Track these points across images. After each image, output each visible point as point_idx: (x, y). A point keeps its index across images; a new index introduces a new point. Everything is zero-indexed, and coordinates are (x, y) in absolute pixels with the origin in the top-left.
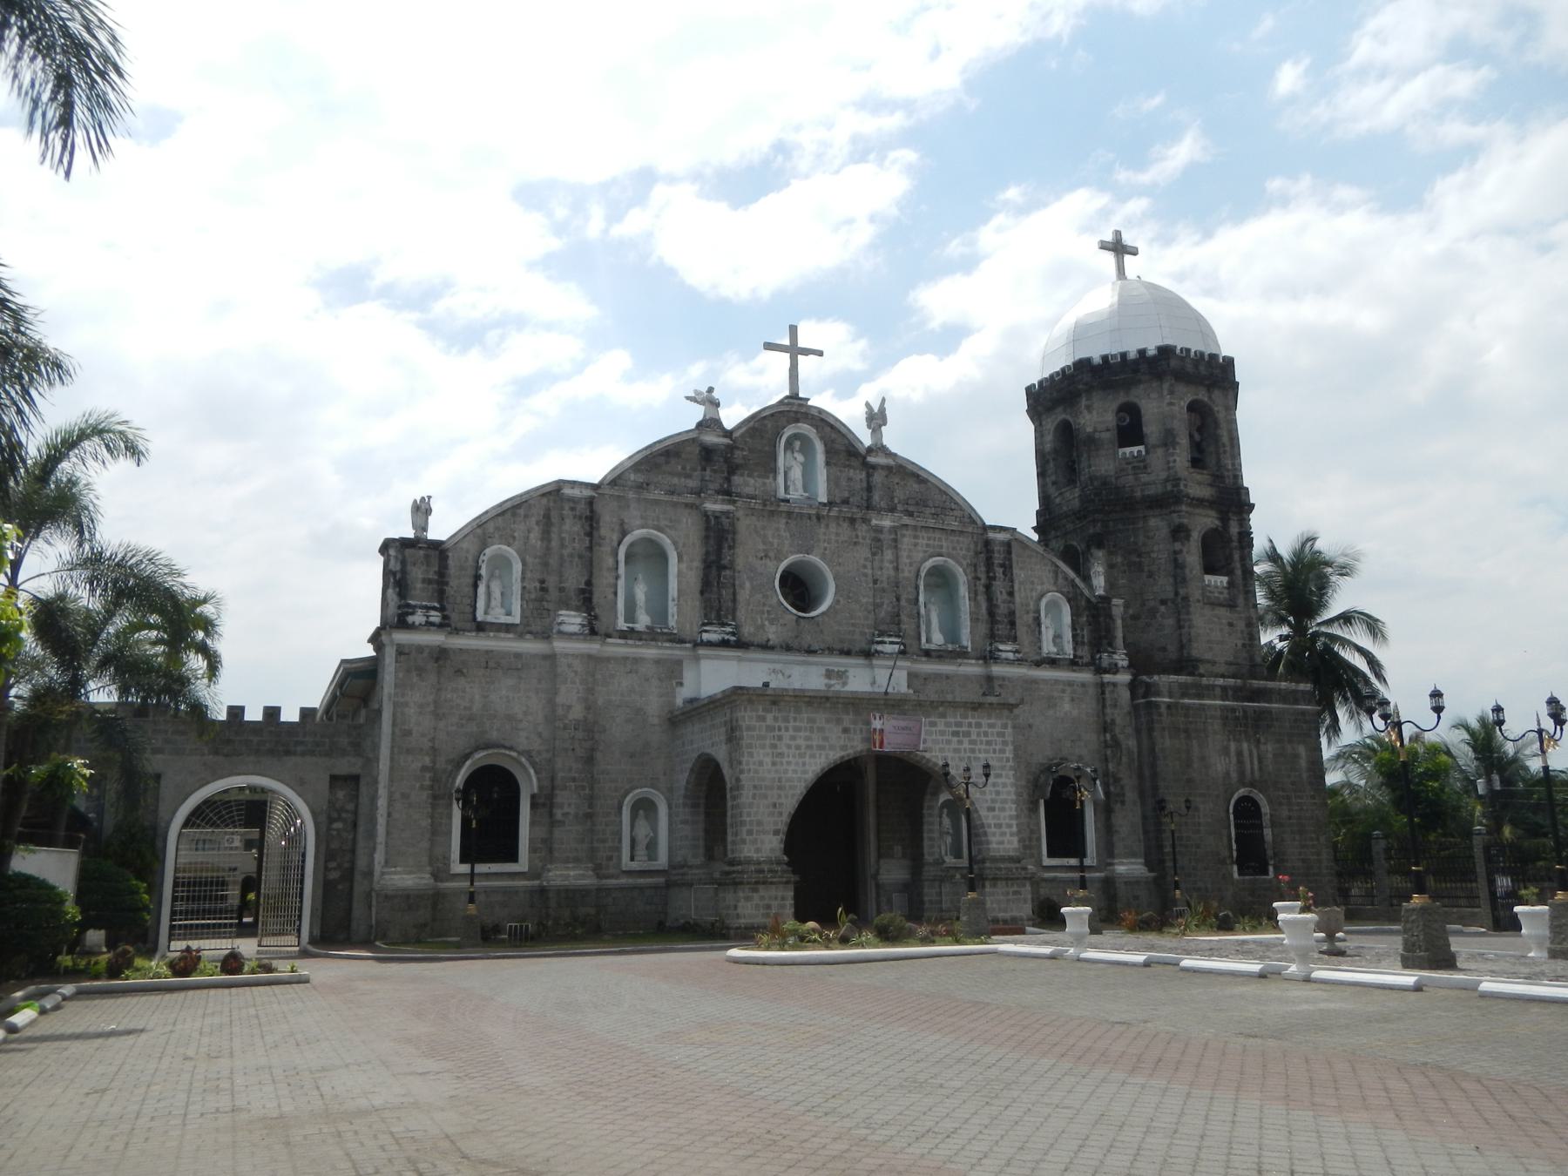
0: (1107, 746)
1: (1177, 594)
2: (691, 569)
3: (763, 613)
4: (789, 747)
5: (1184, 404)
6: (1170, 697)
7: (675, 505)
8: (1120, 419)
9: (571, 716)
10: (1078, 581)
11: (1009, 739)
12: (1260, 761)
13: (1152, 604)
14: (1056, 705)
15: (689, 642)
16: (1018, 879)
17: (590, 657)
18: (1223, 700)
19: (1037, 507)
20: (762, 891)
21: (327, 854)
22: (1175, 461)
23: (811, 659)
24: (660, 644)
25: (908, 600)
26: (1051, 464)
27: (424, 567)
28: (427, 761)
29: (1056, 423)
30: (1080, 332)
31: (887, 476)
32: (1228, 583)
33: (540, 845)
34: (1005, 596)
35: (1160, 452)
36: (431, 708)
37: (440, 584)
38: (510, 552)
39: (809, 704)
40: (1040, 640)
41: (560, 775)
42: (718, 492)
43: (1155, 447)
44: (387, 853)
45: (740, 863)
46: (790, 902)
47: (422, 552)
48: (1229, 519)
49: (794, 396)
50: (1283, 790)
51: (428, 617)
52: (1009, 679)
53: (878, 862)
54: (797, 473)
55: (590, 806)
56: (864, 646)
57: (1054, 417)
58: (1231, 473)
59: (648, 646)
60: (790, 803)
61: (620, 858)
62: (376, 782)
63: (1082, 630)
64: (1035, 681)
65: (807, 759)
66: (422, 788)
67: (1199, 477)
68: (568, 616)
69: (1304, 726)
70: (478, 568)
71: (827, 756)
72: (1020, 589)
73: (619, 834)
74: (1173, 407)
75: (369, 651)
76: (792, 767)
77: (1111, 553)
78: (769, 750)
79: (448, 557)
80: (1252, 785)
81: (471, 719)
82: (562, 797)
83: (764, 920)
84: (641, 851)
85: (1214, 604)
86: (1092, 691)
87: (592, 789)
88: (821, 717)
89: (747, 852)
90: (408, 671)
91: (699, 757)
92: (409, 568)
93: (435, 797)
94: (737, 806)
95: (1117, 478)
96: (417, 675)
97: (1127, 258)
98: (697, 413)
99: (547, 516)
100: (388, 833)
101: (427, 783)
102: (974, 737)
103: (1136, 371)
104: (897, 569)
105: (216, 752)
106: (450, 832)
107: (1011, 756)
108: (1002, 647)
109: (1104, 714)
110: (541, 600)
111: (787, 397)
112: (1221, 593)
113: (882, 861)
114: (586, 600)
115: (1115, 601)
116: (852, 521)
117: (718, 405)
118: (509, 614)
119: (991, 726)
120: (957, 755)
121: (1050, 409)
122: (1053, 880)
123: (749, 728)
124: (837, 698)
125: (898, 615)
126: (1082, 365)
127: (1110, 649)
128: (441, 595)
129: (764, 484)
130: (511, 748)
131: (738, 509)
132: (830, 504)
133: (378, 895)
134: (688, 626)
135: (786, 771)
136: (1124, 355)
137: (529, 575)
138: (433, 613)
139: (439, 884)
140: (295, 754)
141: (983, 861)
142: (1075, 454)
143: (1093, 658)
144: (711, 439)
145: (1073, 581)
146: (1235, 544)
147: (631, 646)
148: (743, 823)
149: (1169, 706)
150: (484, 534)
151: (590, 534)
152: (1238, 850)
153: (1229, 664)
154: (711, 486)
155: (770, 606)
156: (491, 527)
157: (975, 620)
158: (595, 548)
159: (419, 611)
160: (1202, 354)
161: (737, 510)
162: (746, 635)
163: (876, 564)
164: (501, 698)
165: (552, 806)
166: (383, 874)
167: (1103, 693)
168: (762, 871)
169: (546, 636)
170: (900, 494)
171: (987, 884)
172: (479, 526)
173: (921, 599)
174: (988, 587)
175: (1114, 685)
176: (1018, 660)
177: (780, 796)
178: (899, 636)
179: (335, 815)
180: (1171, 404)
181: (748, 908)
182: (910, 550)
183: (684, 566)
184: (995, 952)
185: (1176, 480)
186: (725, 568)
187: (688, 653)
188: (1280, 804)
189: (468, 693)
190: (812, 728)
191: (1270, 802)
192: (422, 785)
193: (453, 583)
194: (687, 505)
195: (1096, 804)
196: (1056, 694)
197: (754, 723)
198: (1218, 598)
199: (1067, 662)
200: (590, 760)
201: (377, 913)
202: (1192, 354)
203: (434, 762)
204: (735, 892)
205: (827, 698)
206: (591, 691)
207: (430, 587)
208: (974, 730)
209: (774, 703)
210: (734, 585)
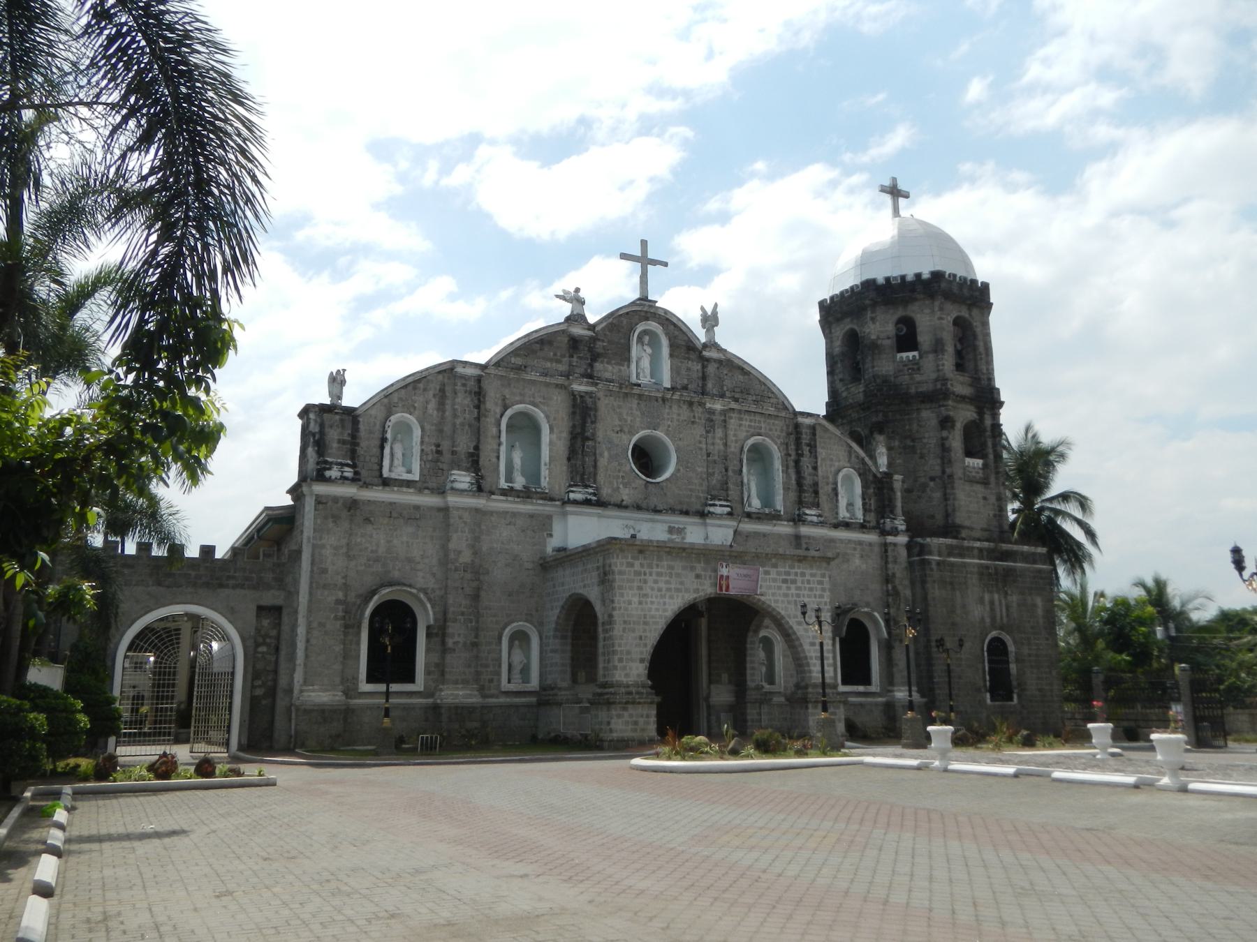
0: (888, 595)
1: (944, 472)
2: (560, 440)
3: (618, 477)
4: (652, 589)
5: (950, 319)
6: (940, 556)
7: (547, 385)
8: (898, 330)
9: (461, 560)
10: (867, 459)
11: (827, 586)
12: (1007, 609)
13: (923, 480)
14: (848, 561)
15: (558, 500)
16: (834, 702)
17: (477, 510)
18: (980, 559)
19: (826, 399)
20: (632, 710)
21: (253, 674)
22: (943, 365)
23: (658, 517)
24: (535, 501)
25: (734, 471)
26: (839, 365)
27: (339, 430)
28: (340, 595)
29: (843, 331)
30: (867, 258)
31: (718, 368)
32: (983, 465)
33: (433, 669)
34: (810, 470)
35: (931, 357)
36: (344, 550)
37: (352, 446)
38: (412, 419)
39: (669, 553)
40: (837, 507)
41: (452, 609)
42: (583, 376)
43: (927, 352)
44: (305, 673)
45: (612, 686)
46: (653, 719)
47: (337, 417)
48: (984, 413)
49: (644, 298)
51: (342, 472)
52: (814, 538)
53: (709, 687)
54: (646, 363)
55: (477, 636)
56: (698, 507)
57: (842, 326)
58: (985, 377)
59: (524, 503)
60: (653, 635)
61: (499, 681)
62: (296, 612)
63: (870, 500)
65: (667, 600)
66: (336, 618)
67: (961, 379)
68: (459, 475)
70: (384, 432)
71: (683, 596)
73: (499, 660)
74: (943, 321)
75: (288, 501)
76: (654, 607)
77: (889, 438)
78: (636, 591)
79: (359, 422)
80: (1002, 628)
81: (377, 560)
82: (453, 628)
83: (634, 734)
84: (516, 676)
85: (972, 481)
86: (877, 549)
87: (477, 622)
88: (678, 565)
89: (619, 676)
90: (326, 518)
91: (570, 596)
92: (327, 430)
93: (346, 627)
94: (610, 638)
95: (895, 377)
96: (333, 522)
97: (902, 201)
98: (566, 309)
99: (442, 390)
100: (307, 656)
101: (340, 614)
102: (799, 584)
103: (913, 291)
104: (726, 445)
105: (159, 584)
106: (359, 656)
107: (828, 600)
108: (808, 512)
109: (887, 569)
110: (437, 461)
111: (639, 299)
112: (978, 473)
113: (712, 686)
114: (474, 463)
115: (896, 477)
116: (691, 404)
117: (583, 303)
118: (409, 472)
119: (813, 575)
120: (786, 599)
121: (839, 320)
123: (621, 573)
124: (692, 549)
125: (727, 483)
126: (869, 285)
127: (891, 516)
128: (353, 454)
129: (620, 370)
130: (410, 586)
131: (599, 390)
132: (673, 389)
133: (297, 710)
134: (557, 487)
135: (650, 610)
136: (903, 277)
137: (426, 439)
138: (346, 469)
139: (349, 700)
140: (227, 586)
141: (806, 687)
142: (859, 357)
143: (878, 523)
144: (577, 331)
145: (863, 459)
146: (988, 433)
147: (511, 502)
148: (614, 652)
149: (938, 563)
150: (390, 403)
151: (478, 407)
152: (990, 681)
153: (986, 530)
154: (578, 370)
155: (624, 472)
156: (395, 398)
157: (786, 489)
158: (482, 419)
159: (335, 467)
160: (965, 279)
161: (598, 391)
162: (605, 495)
163: (710, 441)
164: (402, 543)
165: (444, 635)
166: (302, 691)
167: (886, 551)
168: (630, 693)
169: (441, 491)
170: (728, 383)
171: (810, 705)
172: (386, 397)
173: (745, 470)
174: (797, 462)
175: (895, 545)
176: (821, 523)
177: (645, 631)
178: (727, 501)
179: (261, 640)
180: (941, 318)
181: (620, 724)
182: (735, 430)
183: (554, 436)
184: (861, 763)
185: (945, 380)
186: (588, 439)
187: (559, 510)
189: (376, 538)
190: (671, 573)
191: (1015, 642)
192: (336, 616)
193: (364, 444)
194: (557, 385)
195: (879, 642)
196: (849, 551)
197: (624, 568)
198: (974, 477)
199: (858, 526)
200: (476, 597)
201: (296, 725)
202: (958, 279)
203: (346, 596)
204: (608, 710)
205: (684, 549)
206: (477, 539)
207: (345, 446)
208: (799, 579)
209: (641, 552)
210: (595, 454)
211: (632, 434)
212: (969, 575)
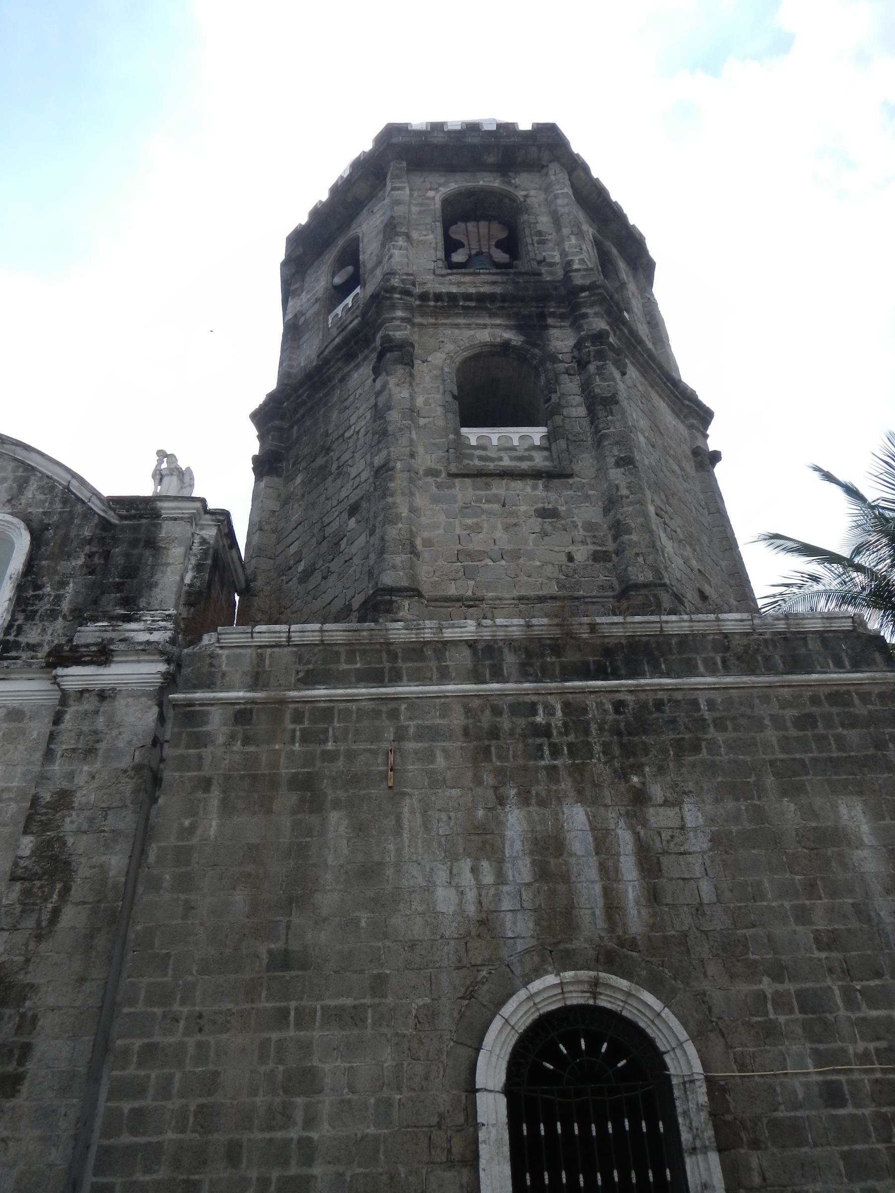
32: (550, 438)
50: (778, 973)
63: (63, 584)
69: (852, 735)
86: (39, 728)
112: (521, 459)
175: (103, 695)
188: (770, 1032)
212: (411, 746)
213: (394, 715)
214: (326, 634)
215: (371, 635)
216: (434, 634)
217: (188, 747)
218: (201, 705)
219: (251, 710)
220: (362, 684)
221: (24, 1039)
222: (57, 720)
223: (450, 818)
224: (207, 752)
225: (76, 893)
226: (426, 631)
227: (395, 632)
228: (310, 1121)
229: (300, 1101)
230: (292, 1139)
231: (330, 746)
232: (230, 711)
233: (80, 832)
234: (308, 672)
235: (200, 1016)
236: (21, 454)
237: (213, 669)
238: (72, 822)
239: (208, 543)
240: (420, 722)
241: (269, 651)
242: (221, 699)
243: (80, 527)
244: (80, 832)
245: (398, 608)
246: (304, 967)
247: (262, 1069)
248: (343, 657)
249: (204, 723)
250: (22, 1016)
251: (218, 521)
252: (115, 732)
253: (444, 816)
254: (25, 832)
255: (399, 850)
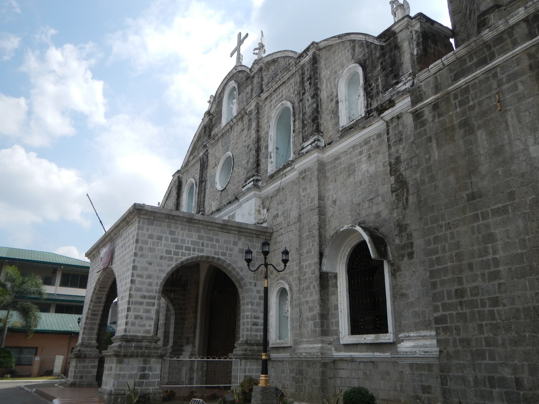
52: (309, 169)
64: (337, 158)
72: (327, 87)
86: (385, 137)
104: (258, 131)
122: (352, 360)
149: (435, 106)
175: (398, 117)
211: (219, 163)
213: (495, 76)
214: (457, 54)
215: (476, 43)
216: (504, 26)
217: (420, 128)
218: (420, 109)
219: (438, 102)
220: (478, 68)
221: (411, 241)
222: (388, 134)
223: (530, 113)
224: (427, 127)
225: (411, 190)
226: (500, 27)
227: (486, 36)
228: (495, 252)
229: (489, 245)
230: (489, 259)
231: (471, 103)
232: (431, 106)
233: (406, 169)
234: (455, 75)
235: (449, 224)
236: (349, 38)
237: (421, 93)
238: (403, 167)
239: (418, 32)
240: (507, 73)
241: (438, 73)
242: (426, 104)
243: (375, 53)
244: (406, 169)
245: (489, 21)
246: (481, 196)
247: (474, 237)
248: (468, 60)
249: (423, 116)
250: (408, 234)
251: (418, 19)
252: (406, 129)
253: (527, 113)
254: (391, 176)
255: (509, 137)
